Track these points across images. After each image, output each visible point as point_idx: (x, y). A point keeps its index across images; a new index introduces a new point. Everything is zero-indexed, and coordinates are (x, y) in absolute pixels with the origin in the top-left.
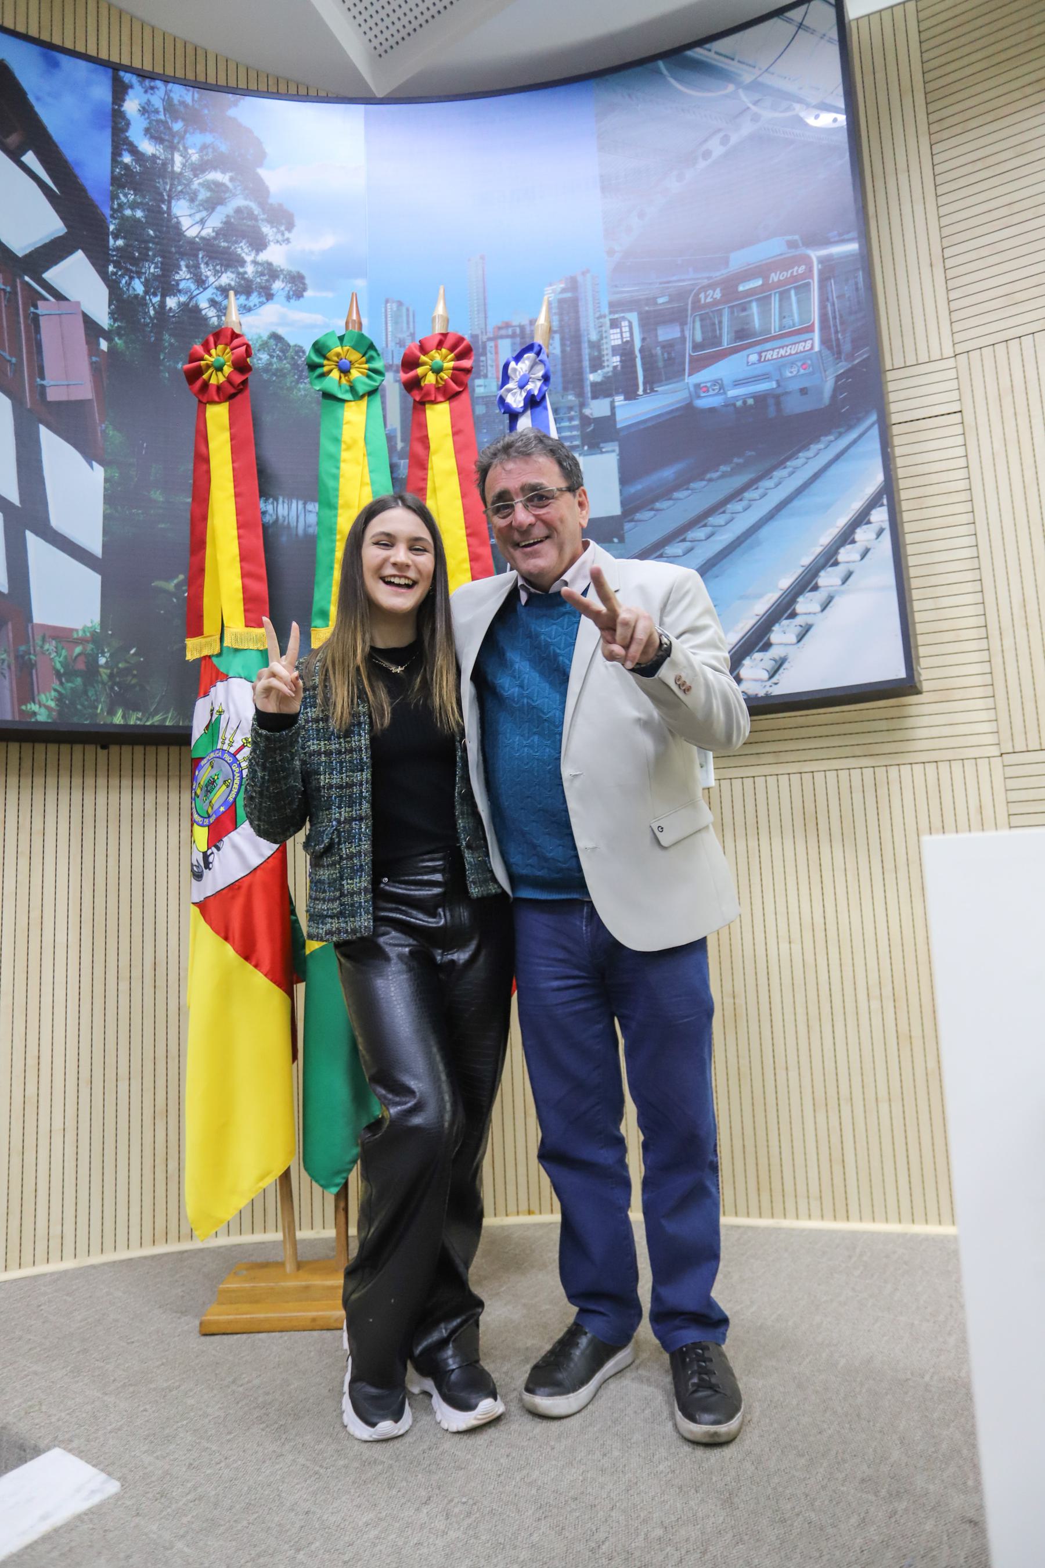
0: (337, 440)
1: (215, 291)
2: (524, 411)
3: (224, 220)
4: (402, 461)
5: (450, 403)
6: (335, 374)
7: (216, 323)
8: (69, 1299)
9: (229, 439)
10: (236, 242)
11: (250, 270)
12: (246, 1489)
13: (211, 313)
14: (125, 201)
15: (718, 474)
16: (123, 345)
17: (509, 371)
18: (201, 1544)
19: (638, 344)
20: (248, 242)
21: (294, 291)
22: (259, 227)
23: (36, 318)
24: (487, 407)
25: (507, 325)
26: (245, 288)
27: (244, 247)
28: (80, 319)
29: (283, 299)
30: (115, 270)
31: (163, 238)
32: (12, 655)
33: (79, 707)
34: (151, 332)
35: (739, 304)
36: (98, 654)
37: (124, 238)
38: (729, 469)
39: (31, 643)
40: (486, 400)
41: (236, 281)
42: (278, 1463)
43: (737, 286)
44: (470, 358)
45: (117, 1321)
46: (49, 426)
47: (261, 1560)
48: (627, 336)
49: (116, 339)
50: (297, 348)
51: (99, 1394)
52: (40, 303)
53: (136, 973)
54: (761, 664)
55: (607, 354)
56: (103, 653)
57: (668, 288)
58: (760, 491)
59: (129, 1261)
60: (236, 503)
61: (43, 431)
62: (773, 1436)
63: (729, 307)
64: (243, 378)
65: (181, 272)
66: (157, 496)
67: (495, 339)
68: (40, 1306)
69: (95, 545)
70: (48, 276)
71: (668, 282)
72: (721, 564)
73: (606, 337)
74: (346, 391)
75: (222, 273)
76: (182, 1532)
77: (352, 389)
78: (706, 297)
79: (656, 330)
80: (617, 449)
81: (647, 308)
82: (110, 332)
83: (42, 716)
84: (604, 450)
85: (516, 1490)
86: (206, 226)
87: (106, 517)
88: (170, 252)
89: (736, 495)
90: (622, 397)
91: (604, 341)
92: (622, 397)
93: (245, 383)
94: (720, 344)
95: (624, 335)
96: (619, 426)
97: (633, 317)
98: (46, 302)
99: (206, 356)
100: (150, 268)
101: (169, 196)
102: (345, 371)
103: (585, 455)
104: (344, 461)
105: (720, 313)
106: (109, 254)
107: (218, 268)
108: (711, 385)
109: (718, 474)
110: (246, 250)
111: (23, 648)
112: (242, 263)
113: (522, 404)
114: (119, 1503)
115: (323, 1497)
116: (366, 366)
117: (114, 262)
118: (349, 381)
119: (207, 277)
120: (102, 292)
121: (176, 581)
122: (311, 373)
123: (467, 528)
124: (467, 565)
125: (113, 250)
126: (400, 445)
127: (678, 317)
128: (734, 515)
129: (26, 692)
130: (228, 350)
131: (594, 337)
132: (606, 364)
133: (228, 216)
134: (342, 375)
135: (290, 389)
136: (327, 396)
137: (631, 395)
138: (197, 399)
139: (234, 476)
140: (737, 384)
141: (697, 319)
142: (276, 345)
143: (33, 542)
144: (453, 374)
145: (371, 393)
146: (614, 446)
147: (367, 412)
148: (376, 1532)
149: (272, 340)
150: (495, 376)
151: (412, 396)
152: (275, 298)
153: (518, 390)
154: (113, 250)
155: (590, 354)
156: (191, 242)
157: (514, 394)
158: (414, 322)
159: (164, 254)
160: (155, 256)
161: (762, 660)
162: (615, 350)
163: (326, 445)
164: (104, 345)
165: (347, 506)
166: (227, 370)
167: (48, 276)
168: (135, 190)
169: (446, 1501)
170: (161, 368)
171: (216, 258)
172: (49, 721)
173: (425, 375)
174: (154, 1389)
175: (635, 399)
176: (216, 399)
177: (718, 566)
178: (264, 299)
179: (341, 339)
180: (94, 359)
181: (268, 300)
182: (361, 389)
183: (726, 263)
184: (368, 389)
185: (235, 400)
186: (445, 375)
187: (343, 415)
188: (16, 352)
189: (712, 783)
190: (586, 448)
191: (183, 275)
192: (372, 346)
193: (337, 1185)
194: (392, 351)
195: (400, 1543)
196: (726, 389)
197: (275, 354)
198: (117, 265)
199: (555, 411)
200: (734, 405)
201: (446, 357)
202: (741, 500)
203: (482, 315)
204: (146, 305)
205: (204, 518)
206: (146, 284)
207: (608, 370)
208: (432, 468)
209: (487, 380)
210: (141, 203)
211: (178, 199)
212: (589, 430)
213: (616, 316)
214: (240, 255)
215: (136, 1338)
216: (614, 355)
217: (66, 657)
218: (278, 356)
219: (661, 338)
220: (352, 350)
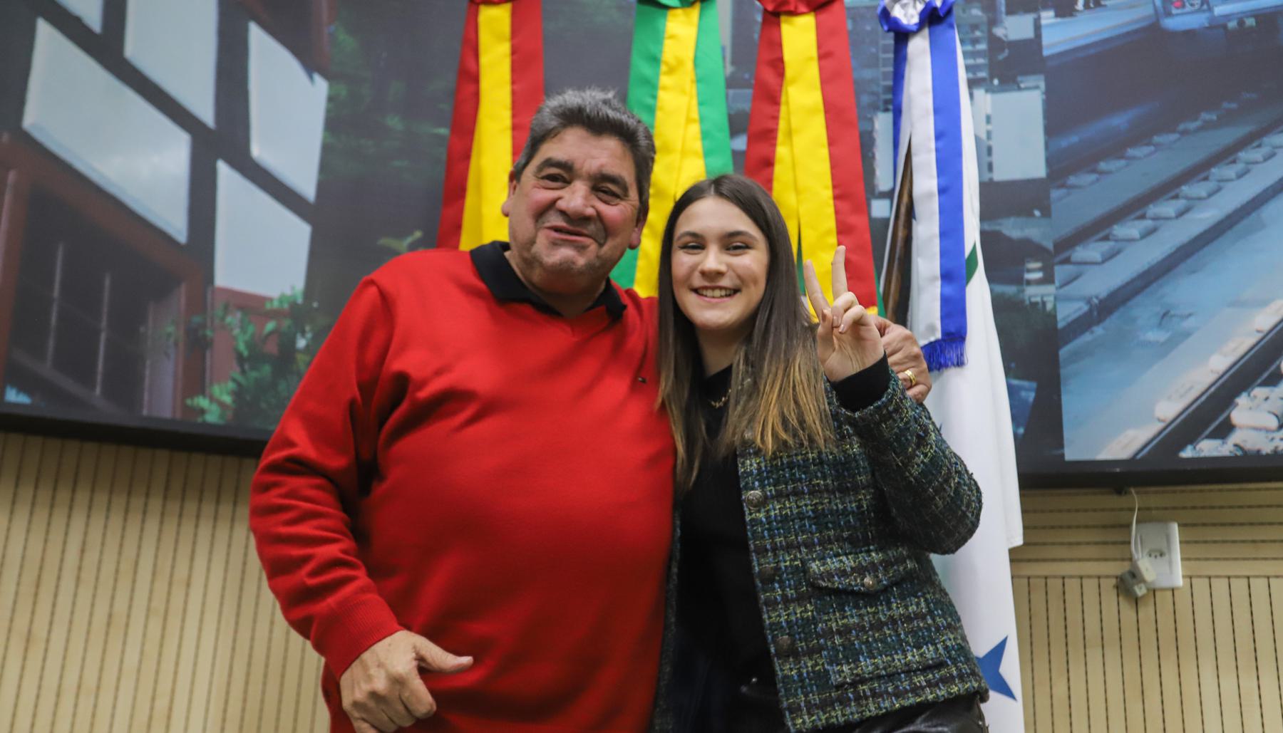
0: (655, 60)
15: (1198, 123)
33: (263, 405)
36: (295, 335)
38: (1214, 117)
54: (1267, 406)
58: (1265, 150)
60: (514, 138)
69: (307, 186)
72: (1201, 253)
80: (1042, 85)
83: (213, 416)
87: (326, 149)
89: (1226, 155)
92: (1051, 13)
96: (1046, 53)
104: (665, 88)
109: (1198, 123)
111: (197, 319)
113: (916, 20)
121: (409, 240)
123: (834, 187)
126: (730, 69)
128: (1222, 184)
129: (195, 381)
161: (1267, 399)
163: (639, 66)
165: (668, 150)
172: (221, 422)
177: (1195, 257)
187: (665, 25)
189: (1179, 581)
190: (996, 82)
196: (1211, 5)
200: (1225, 27)
202: (1234, 162)
205: (466, 156)
208: (787, 103)
212: (1001, 57)
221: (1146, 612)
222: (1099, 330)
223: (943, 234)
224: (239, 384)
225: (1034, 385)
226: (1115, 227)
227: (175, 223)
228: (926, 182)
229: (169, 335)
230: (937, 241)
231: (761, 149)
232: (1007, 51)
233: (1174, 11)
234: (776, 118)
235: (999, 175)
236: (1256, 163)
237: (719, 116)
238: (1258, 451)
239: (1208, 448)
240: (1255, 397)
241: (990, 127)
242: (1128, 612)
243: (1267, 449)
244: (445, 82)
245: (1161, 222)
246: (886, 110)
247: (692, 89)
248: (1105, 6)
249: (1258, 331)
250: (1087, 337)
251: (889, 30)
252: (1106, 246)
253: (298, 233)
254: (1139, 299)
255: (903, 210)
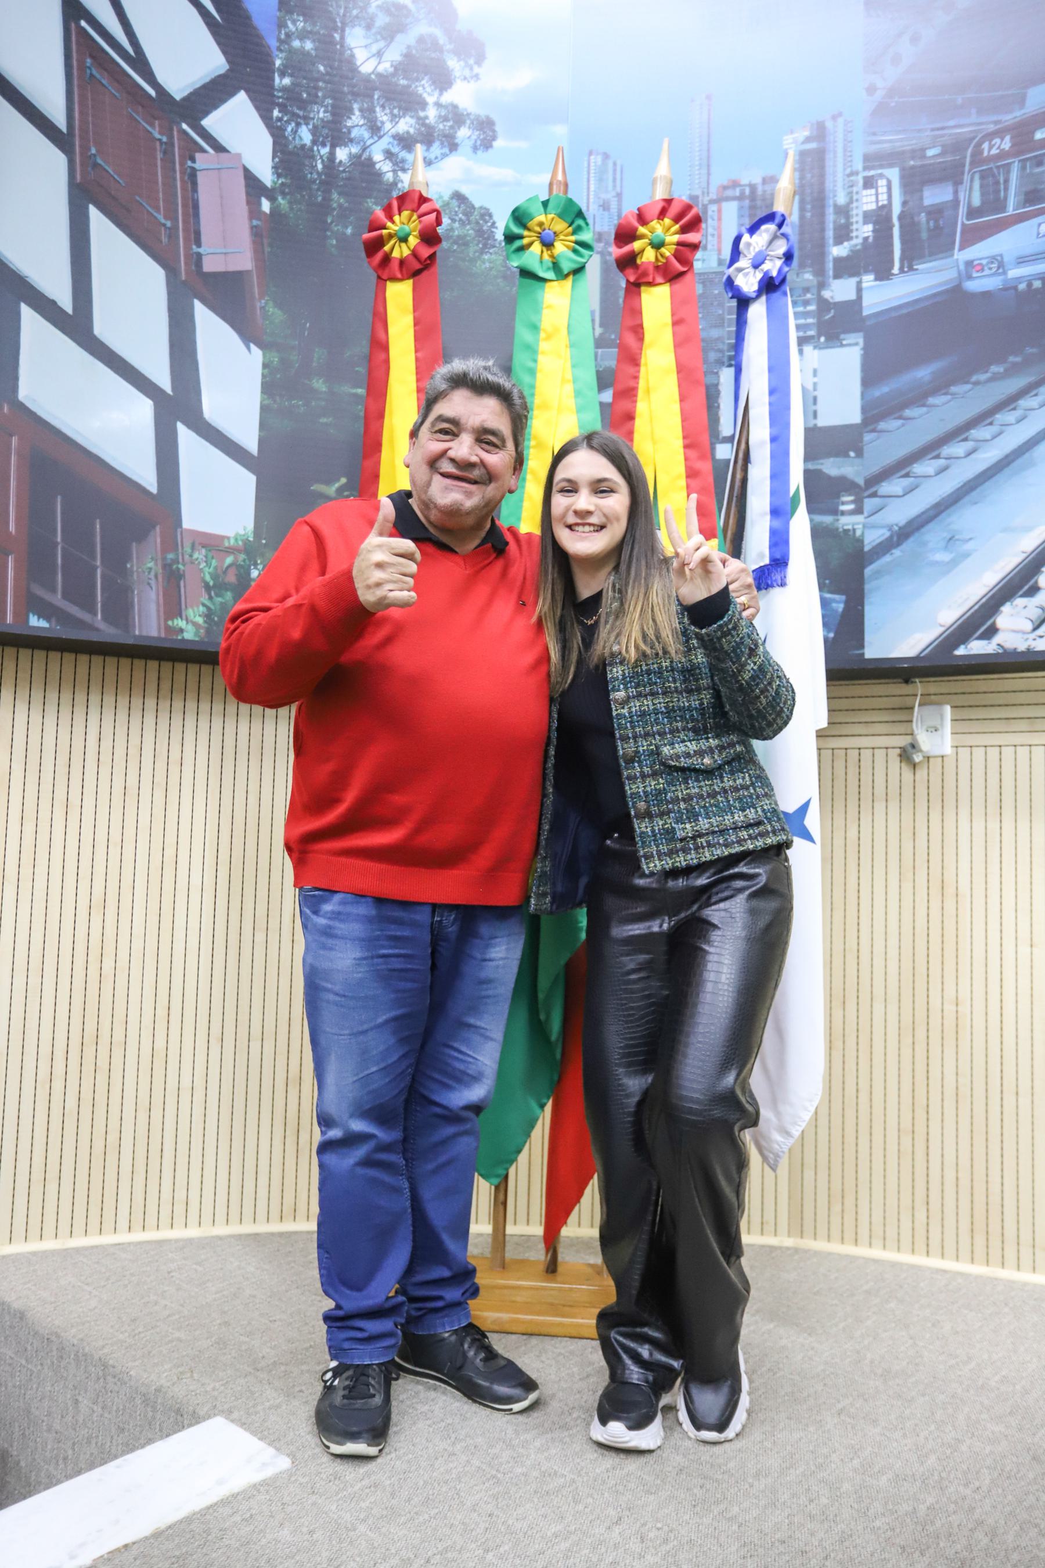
0: (535, 328)
1: (391, 140)
2: (758, 296)
3: (405, 51)
4: (600, 351)
5: (671, 285)
6: (537, 247)
7: (391, 180)
8: (200, 1269)
9: (412, 323)
10: (417, 80)
11: (431, 114)
12: (422, 1483)
13: (385, 167)
14: (294, 30)
15: (988, 375)
16: (287, 205)
17: (742, 246)
18: (384, 1530)
19: (896, 209)
20: (431, 79)
21: (482, 140)
22: (444, 61)
23: (193, 174)
24: (705, 286)
25: (735, 184)
26: (427, 137)
27: (426, 85)
28: (241, 173)
29: (469, 150)
30: (280, 115)
31: (335, 76)
32: (160, 562)
34: (318, 190)
35: (1035, 157)
36: (249, 566)
37: (291, 75)
38: (1002, 370)
39: (180, 550)
40: (707, 279)
41: (415, 128)
42: (452, 1462)
43: (1033, 133)
44: (698, 231)
45: (254, 1296)
46: (204, 301)
47: (449, 1555)
48: (883, 199)
49: (280, 198)
50: (482, 211)
51: (250, 1369)
52: (198, 156)
53: (274, 924)
55: (857, 222)
56: (256, 565)
57: (942, 136)
59: (256, 1236)
61: (198, 306)
62: (1008, 1509)
63: (1019, 161)
64: (431, 251)
65: (354, 118)
66: (319, 384)
67: (718, 201)
68: (169, 1273)
69: (251, 443)
70: (207, 122)
71: (943, 128)
73: (857, 200)
74: (549, 269)
75: (400, 118)
76: (362, 1516)
77: (556, 266)
78: (991, 148)
79: (922, 191)
80: (861, 341)
81: (912, 163)
82: (273, 189)
83: (190, 634)
84: (844, 342)
85: (715, 1524)
86: (383, 59)
87: (264, 409)
88: (342, 93)
89: (1009, 402)
90: (872, 277)
91: (855, 205)
92: (872, 277)
93: (432, 257)
94: (1003, 209)
95: (880, 197)
96: (865, 313)
97: (894, 174)
98: (205, 155)
99: (389, 224)
100: (318, 112)
101: (342, 23)
102: (548, 244)
103: (820, 348)
105: (1007, 168)
106: (275, 96)
107: (396, 111)
108: (988, 263)
109: (988, 375)
110: (428, 89)
111: (171, 556)
112: (424, 105)
113: (756, 287)
114: (293, 1479)
115: (504, 1502)
116: (573, 238)
117: (279, 105)
118: (552, 256)
119: (383, 123)
120: (267, 141)
121: (337, 485)
122: (508, 246)
123: (684, 438)
124: (683, 482)
125: (279, 91)
126: (599, 331)
127: (951, 174)
128: (1003, 428)
129: (173, 607)
130: (415, 217)
131: (841, 199)
132: (854, 234)
133: (409, 47)
134: (545, 249)
135: (473, 261)
136: (526, 274)
137: (883, 274)
138: (375, 275)
139: (417, 368)
140: (1021, 261)
141: (977, 177)
142: (459, 207)
143: (184, 434)
144: (676, 250)
145: (578, 271)
146: (859, 338)
147: (572, 295)
148: (567, 1545)
149: (454, 201)
150: (716, 247)
151: (625, 275)
152: (460, 149)
153: (751, 270)
154: (279, 91)
155: (835, 222)
156: (367, 79)
157: (747, 274)
158: (622, 179)
159: (336, 95)
160: (325, 97)
161: (1025, 607)
162: (867, 217)
163: (522, 333)
164: (266, 206)
166: (413, 241)
167: (207, 122)
168: (304, 15)
169: (638, 1524)
170: (329, 233)
171: (394, 100)
173: (642, 251)
174: (308, 1371)
175: (888, 279)
176: (399, 276)
177: (978, 490)
178: (446, 150)
179: (545, 204)
180: (255, 222)
181: (451, 151)
182: (566, 266)
183: (1022, 101)
184: (575, 266)
185: (417, 278)
186: (667, 252)
187: (543, 297)
188: (172, 215)
189: (948, 750)
190: (822, 339)
191: (356, 120)
192: (580, 214)
193: (497, 1176)
194: (594, 216)
195: (595, 1559)
196: (1006, 268)
197: (457, 218)
198: (283, 108)
199: (792, 296)
200: (1015, 288)
201: (669, 229)
202: (1014, 409)
203: (704, 171)
204: (313, 157)
205: (381, 416)
206: (314, 132)
207: (857, 242)
208: (646, 364)
209: (706, 253)
210: (310, 32)
211: (353, 27)
212: (827, 317)
213: (872, 173)
214: (421, 95)
215: (278, 1317)
216: (865, 223)
217: (216, 568)
218: (461, 220)
219: (927, 202)
220: (557, 219)
221: (922, 773)
222: (897, 552)
223: (774, 476)
224: (208, 608)
225: (843, 598)
226: (915, 465)
227: (146, 476)
228: (760, 433)
229: (150, 569)
230: (768, 482)
231: (624, 405)
232: (832, 311)
233: (975, 275)
234: (636, 378)
235: (822, 422)
236: (1034, 409)
237: (590, 378)
238: (1015, 649)
239: (976, 647)
240: (1017, 606)
241: (816, 380)
242: (907, 774)
243: (1022, 647)
244: (362, 347)
245: (953, 460)
246: (730, 366)
247: (566, 353)
248: (917, 270)
249: (1023, 552)
250: (887, 558)
251: (732, 298)
252: (907, 482)
253: (246, 482)
254: (931, 526)
255: (741, 455)
